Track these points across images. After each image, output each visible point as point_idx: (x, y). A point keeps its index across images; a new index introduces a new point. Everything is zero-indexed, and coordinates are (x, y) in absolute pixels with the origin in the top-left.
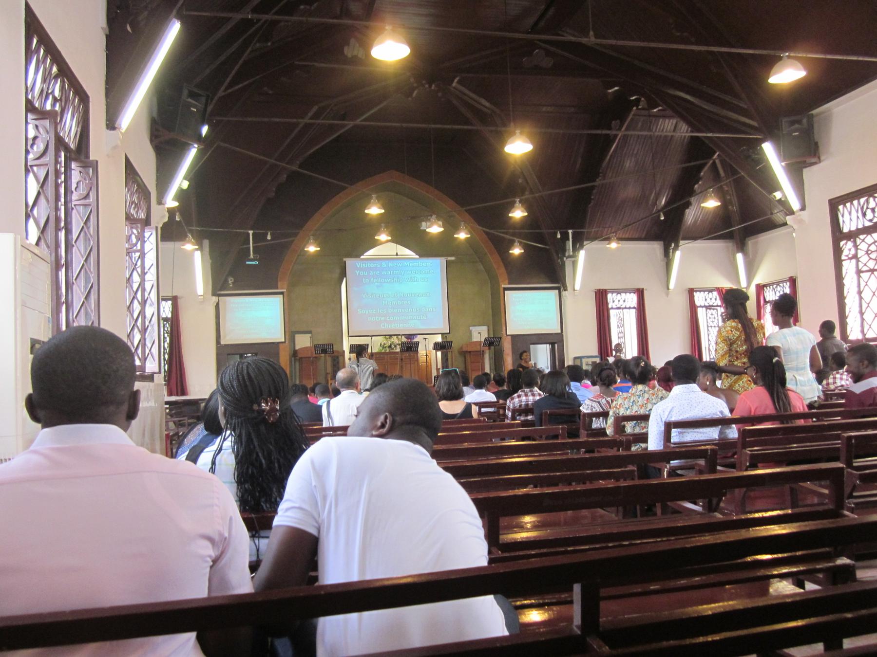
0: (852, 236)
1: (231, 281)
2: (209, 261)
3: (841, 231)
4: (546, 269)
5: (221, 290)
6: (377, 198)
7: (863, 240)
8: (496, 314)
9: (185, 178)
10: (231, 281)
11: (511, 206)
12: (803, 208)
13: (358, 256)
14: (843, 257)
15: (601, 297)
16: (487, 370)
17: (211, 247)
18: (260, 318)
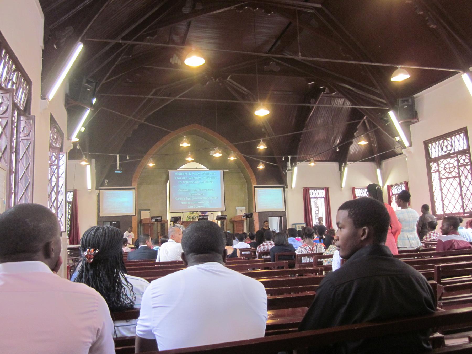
0: (436, 160)
1: (106, 181)
2: (95, 171)
3: (430, 158)
4: (277, 176)
5: (101, 186)
6: (186, 138)
7: (442, 162)
8: (250, 200)
9: (83, 126)
10: (106, 181)
11: (258, 143)
12: (411, 145)
13: (176, 169)
14: (432, 171)
15: (306, 191)
16: (245, 231)
17: (96, 163)
18: (121, 202)
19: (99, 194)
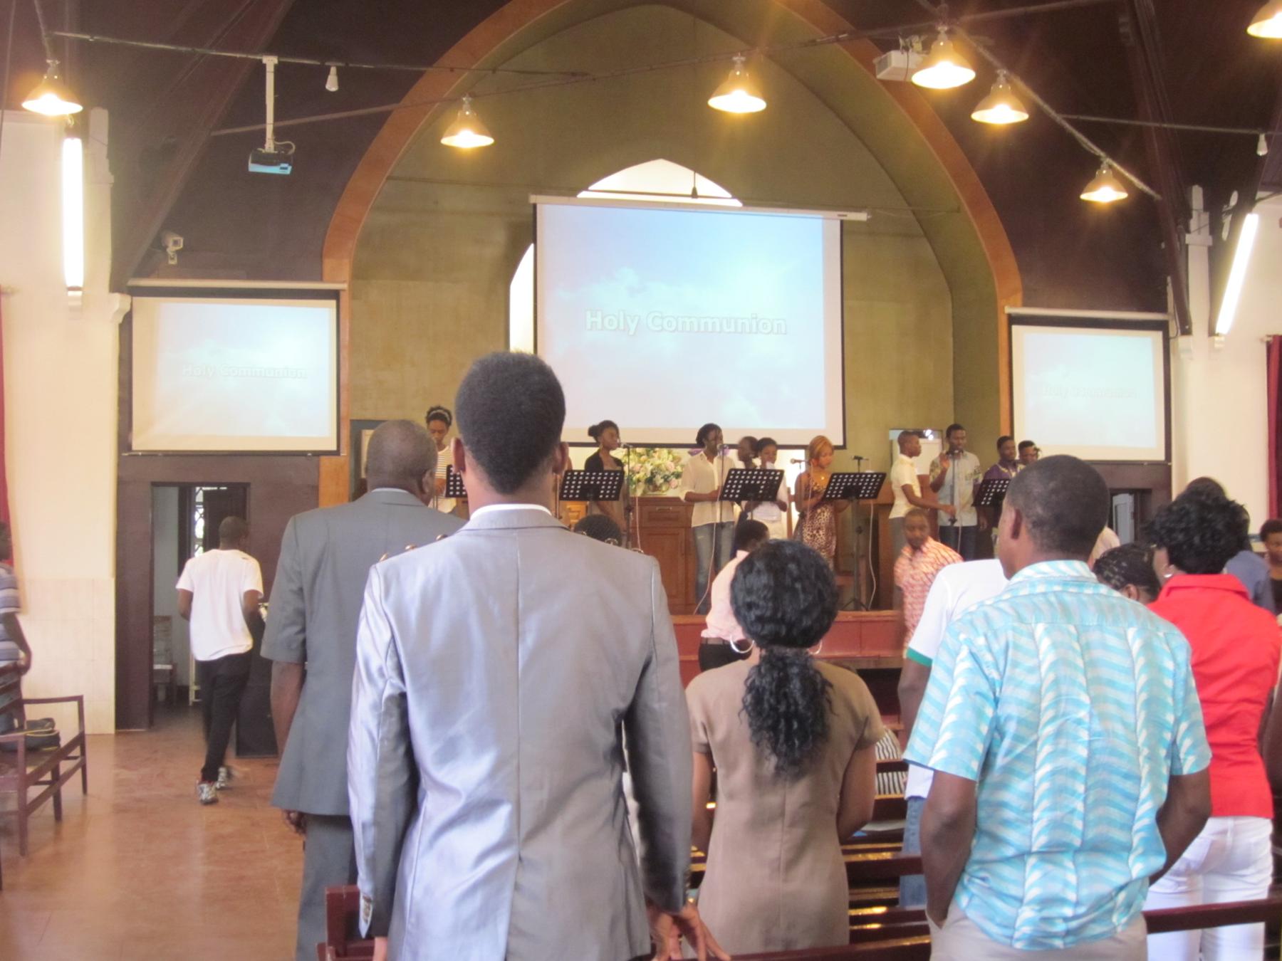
5: (140, 274)
8: (976, 393)
10: (174, 244)
13: (572, 191)
17: (114, 133)
18: (264, 369)
19: (128, 318)
